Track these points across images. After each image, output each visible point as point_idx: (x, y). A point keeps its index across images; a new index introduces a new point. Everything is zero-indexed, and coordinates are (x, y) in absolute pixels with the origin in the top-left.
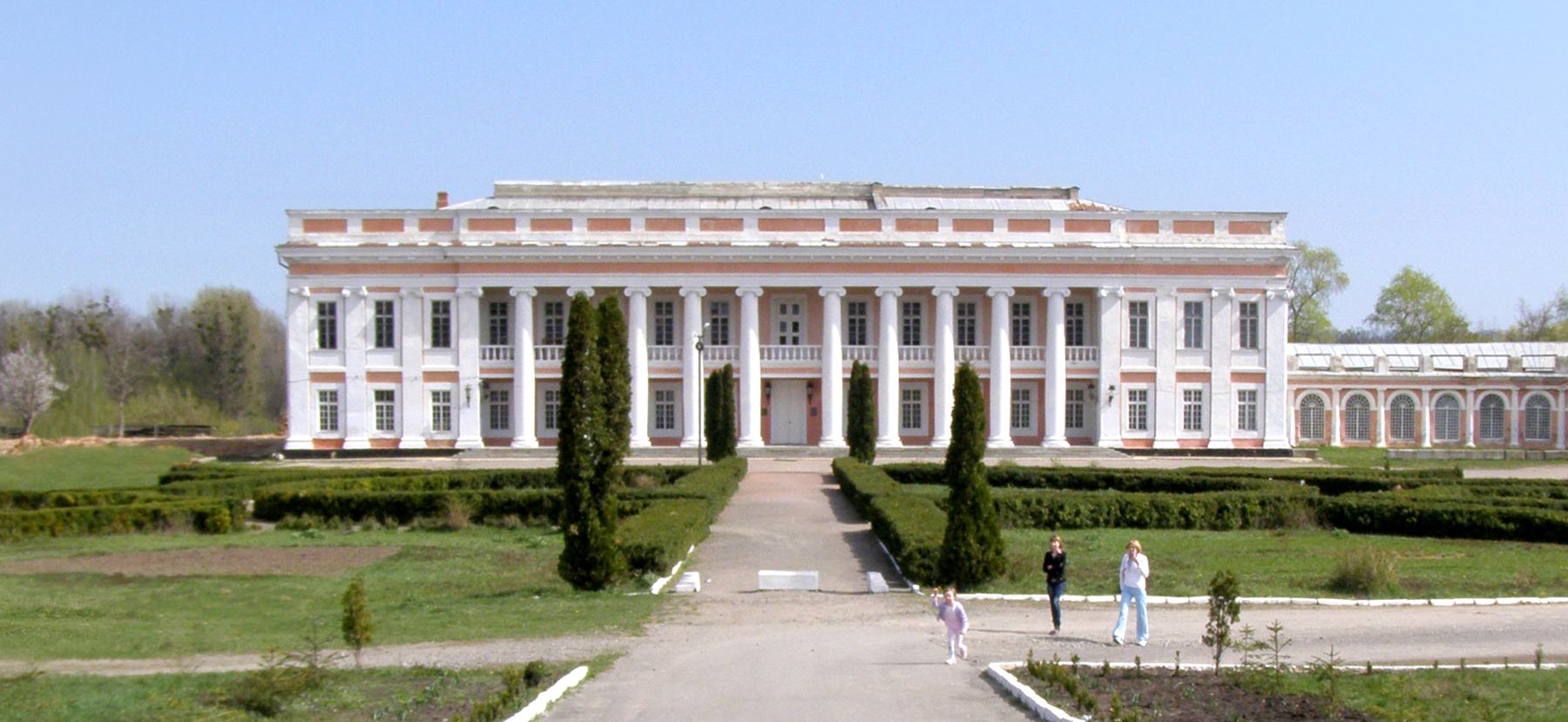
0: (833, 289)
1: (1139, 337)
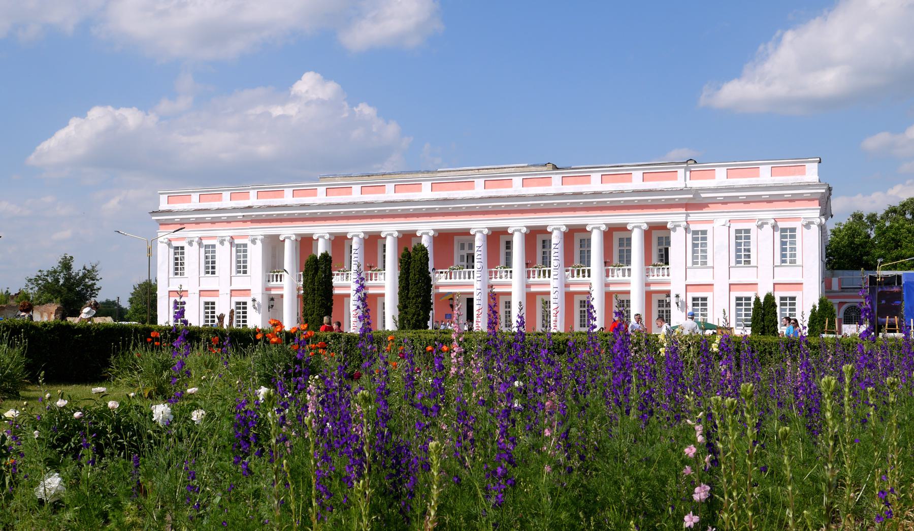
0: (479, 227)
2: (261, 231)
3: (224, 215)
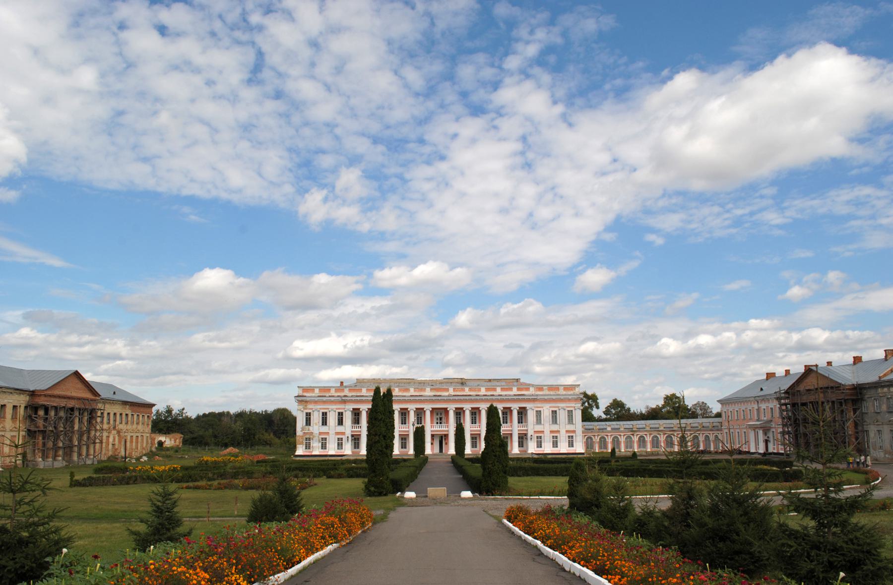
0: (451, 407)
1: (539, 420)
2: (351, 407)
3: (332, 399)
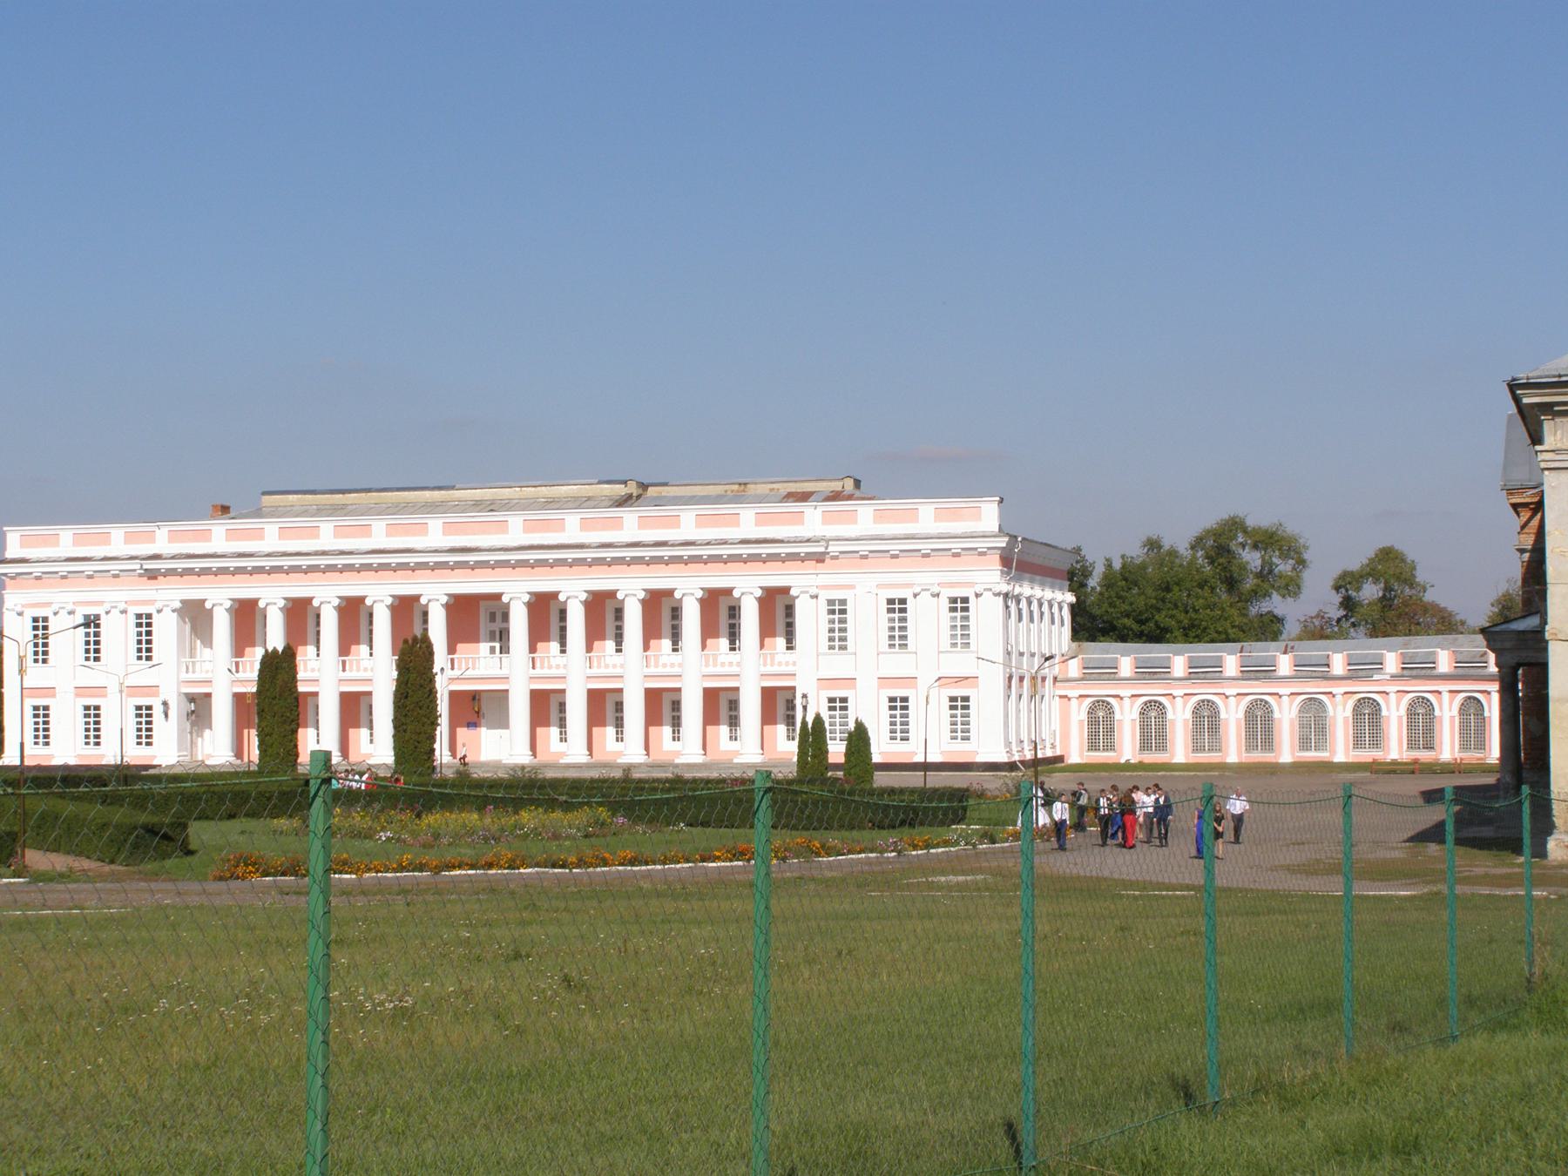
0: (516, 591)
